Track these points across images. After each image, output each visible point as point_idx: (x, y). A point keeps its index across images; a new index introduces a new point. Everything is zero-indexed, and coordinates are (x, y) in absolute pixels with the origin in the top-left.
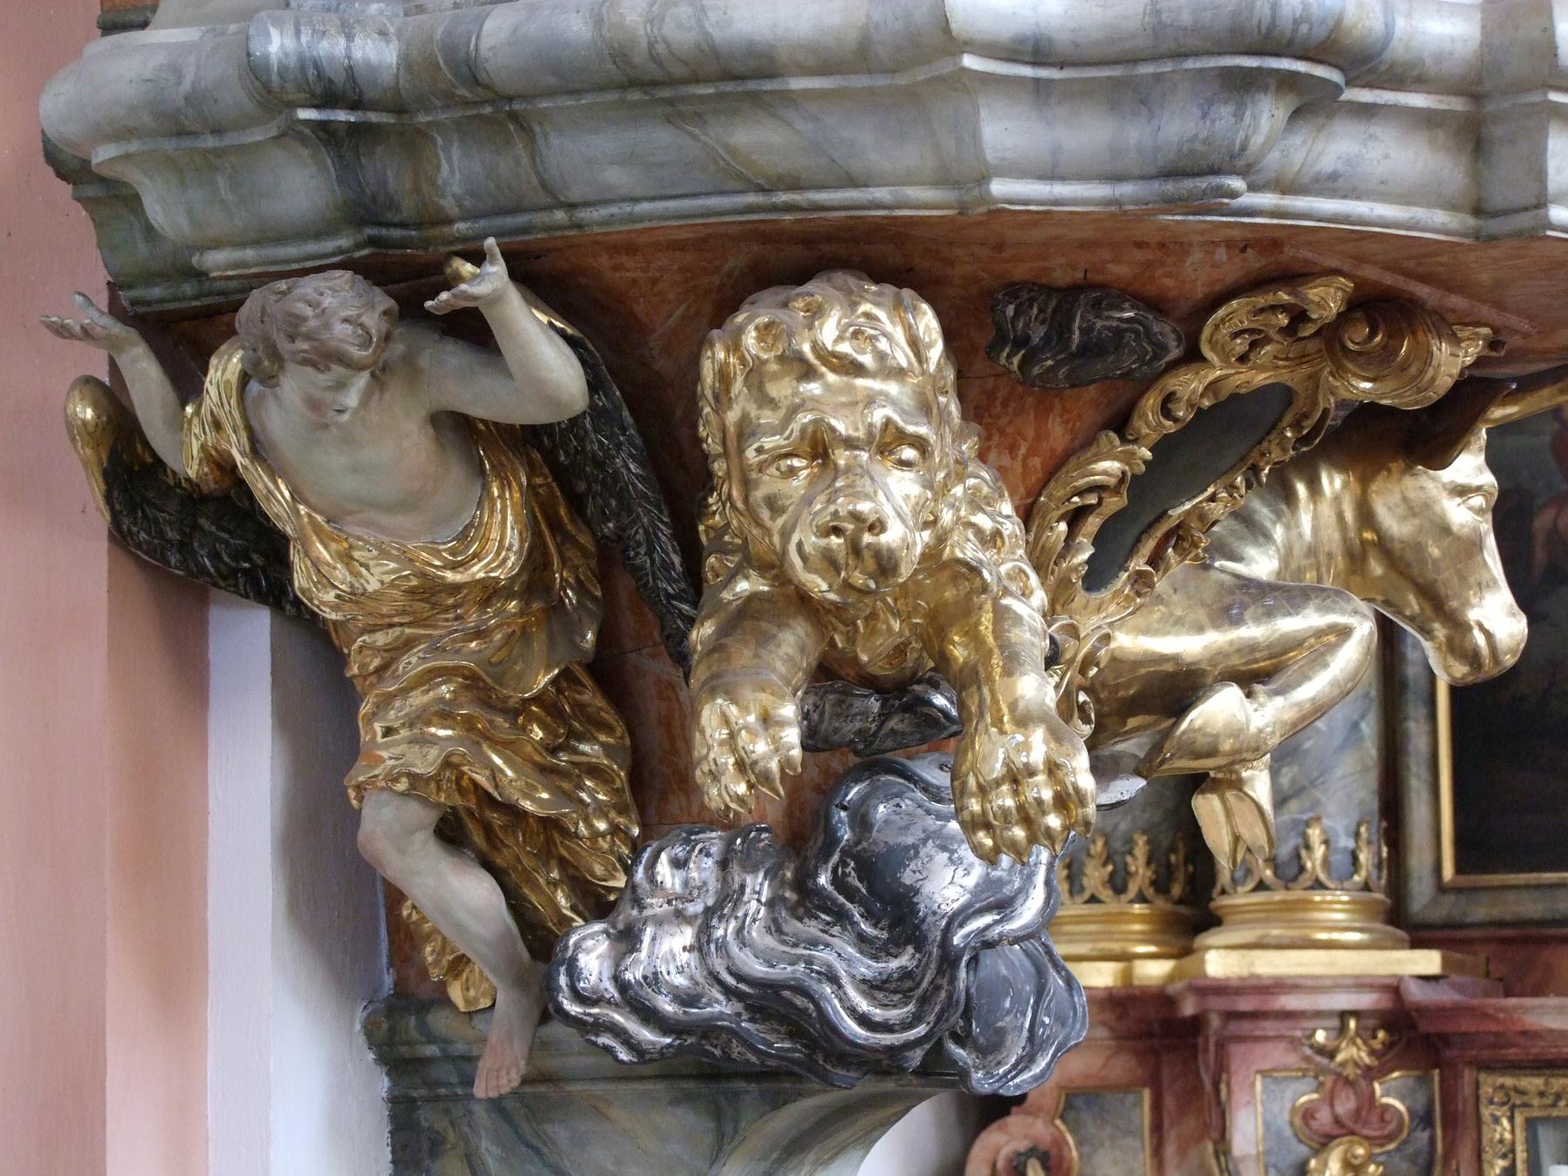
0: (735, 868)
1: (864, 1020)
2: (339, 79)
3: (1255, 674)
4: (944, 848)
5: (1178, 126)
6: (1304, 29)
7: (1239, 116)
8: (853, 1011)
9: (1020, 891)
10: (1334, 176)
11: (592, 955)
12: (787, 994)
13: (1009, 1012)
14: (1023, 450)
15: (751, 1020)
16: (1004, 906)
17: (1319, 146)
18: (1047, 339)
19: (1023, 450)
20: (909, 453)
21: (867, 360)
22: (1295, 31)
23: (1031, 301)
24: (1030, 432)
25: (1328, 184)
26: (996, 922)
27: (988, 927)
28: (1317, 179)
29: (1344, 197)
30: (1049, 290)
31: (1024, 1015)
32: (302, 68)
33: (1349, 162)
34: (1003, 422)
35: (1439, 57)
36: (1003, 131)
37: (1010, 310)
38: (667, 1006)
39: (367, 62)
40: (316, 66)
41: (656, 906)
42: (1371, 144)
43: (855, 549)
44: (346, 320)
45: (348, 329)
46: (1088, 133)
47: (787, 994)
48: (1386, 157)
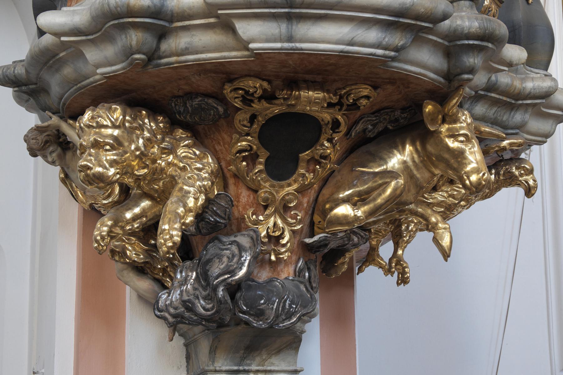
1: (204, 308)
2: (14, 79)
4: (218, 258)
6: (119, 9)
7: (126, 37)
8: (201, 306)
9: (236, 268)
10: (187, 49)
12: (188, 304)
13: (263, 304)
14: (222, 144)
15: (187, 312)
16: (233, 273)
17: (178, 41)
18: (184, 110)
19: (222, 144)
20: (108, 147)
21: (95, 125)
22: (117, 10)
23: (177, 100)
24: (220, 138)
25: (186, 51)
26: (228, 278)
27: (226, 279)
28: (182, 50)
29: (197, 54)
30: (179, 97)
31: (274, 305)
32: (4, 78)
33: (188, 44)
34: (212, 136)
35: (190, 8)
36: (92, 55)
37: (173, 105)
39: (18, 73)
40: (7, 76)
41: (176, 284)
42: (194, 37)
43: (87, 175)
44: (33, 139)
45: (34, 141)
46: (109, 51)
47: (188, 304)
48: (200, 40)
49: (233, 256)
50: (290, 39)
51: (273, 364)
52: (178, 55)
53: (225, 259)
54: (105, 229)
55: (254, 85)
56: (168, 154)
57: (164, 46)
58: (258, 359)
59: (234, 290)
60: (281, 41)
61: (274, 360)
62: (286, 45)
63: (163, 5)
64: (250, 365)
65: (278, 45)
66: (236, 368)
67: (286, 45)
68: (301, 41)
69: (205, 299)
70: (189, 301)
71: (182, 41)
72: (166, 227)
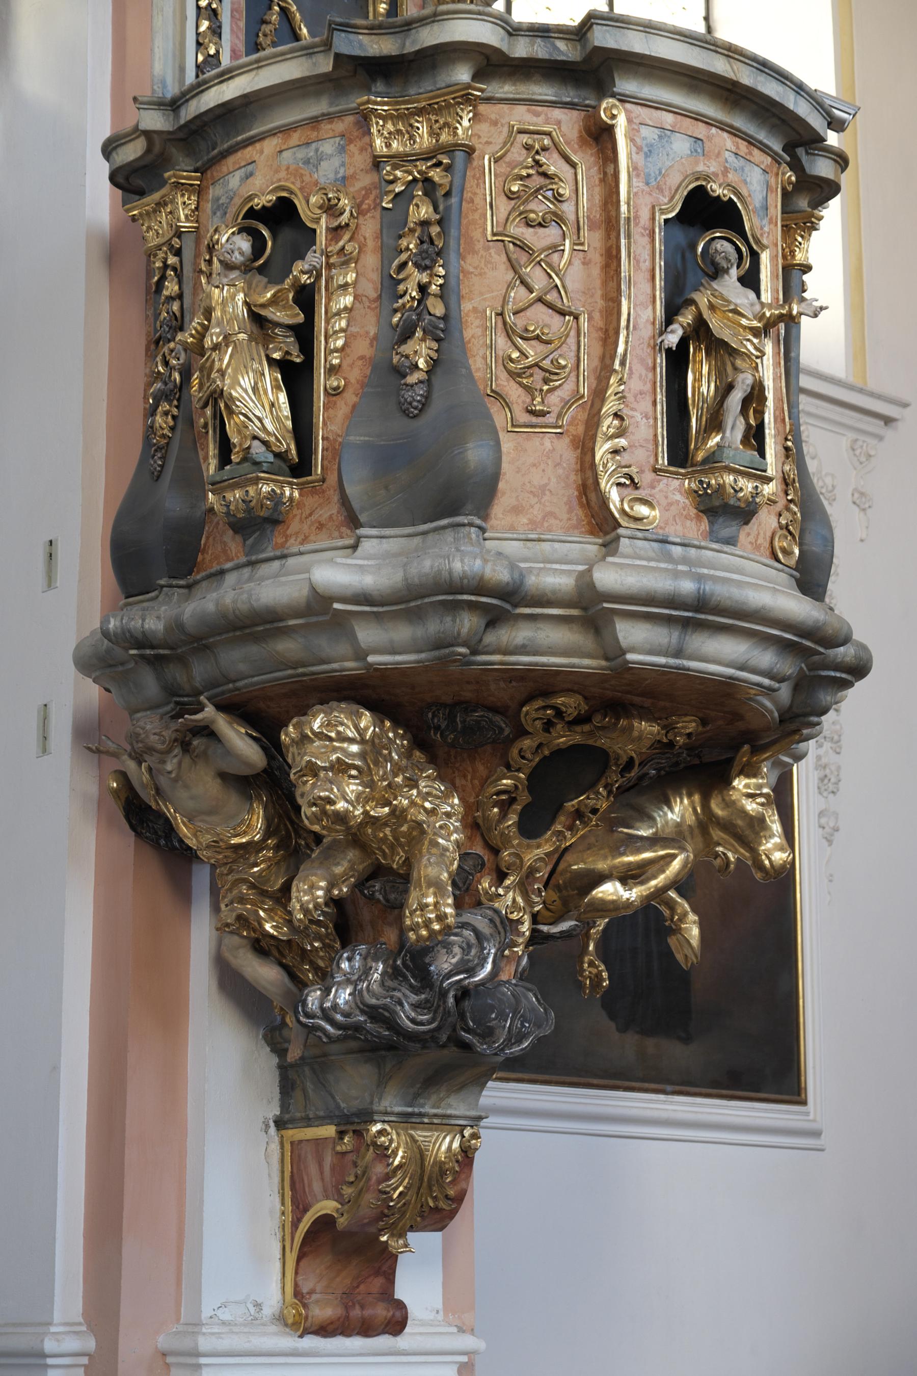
0: (369, 960)
1: (413, 1021)
2: (140, 636)
3: (629, 877)
4: (444, 947)
5: (434, 627)
6: (465, 581)
7: (454, 621)
8: (408, 1017)
9: (477, 965)
10: (524, 646)
11: (313, 999)
12: (380, 1010)
13: (494, 1019)
14: (469, 777)
15: (371, 1023)
16: (471, 971)
17: (514, 634)
18: (448, 726)
19: (469, 777)
20: (354, 772)
21: (333, 735)
22: (462, 582)
23: (438, 710)
24: (470, 769)
26: (465, 978)
27: (461, 980)
28: (516, 647)
29: (534, 655)
30: (444, 705)
31: (506, 1022)
32: (124, 633)
33: (529, 640)
34: (457, 765)
35: (554, 592)
36: (367, 634)
37: (430, 715)
38: (339, 1017)
39: (150, 629)
40: (129, 631)
41: (339, 978)
42: (539, 632)
43: (324, 812)
44: (155, 734)
45: (157, 737)
46: (402, 633)
47: (380, 1010)
48: (548, 637)
49: (469, 946)
50: (678, 653)
51: (450, 1106)
52: (506, 653)
53: (456, 950)
54: (320, 893)
55: (569, 703)
56: (411, 788)
57: (490, 638)
58: (434, 1098)
59: (464, 993)
60: (666, 655)
61: (452, 1100)
62: (672, 661)
63: (522, 583)
64: (422, 1106)
65: (662, 660)
66: (410, 1110)
67: (672, 661)
68: (690, 658)
69: (415, 1006)
70: (385, 1007)
71: (522, 634)
72: (430, 900)
